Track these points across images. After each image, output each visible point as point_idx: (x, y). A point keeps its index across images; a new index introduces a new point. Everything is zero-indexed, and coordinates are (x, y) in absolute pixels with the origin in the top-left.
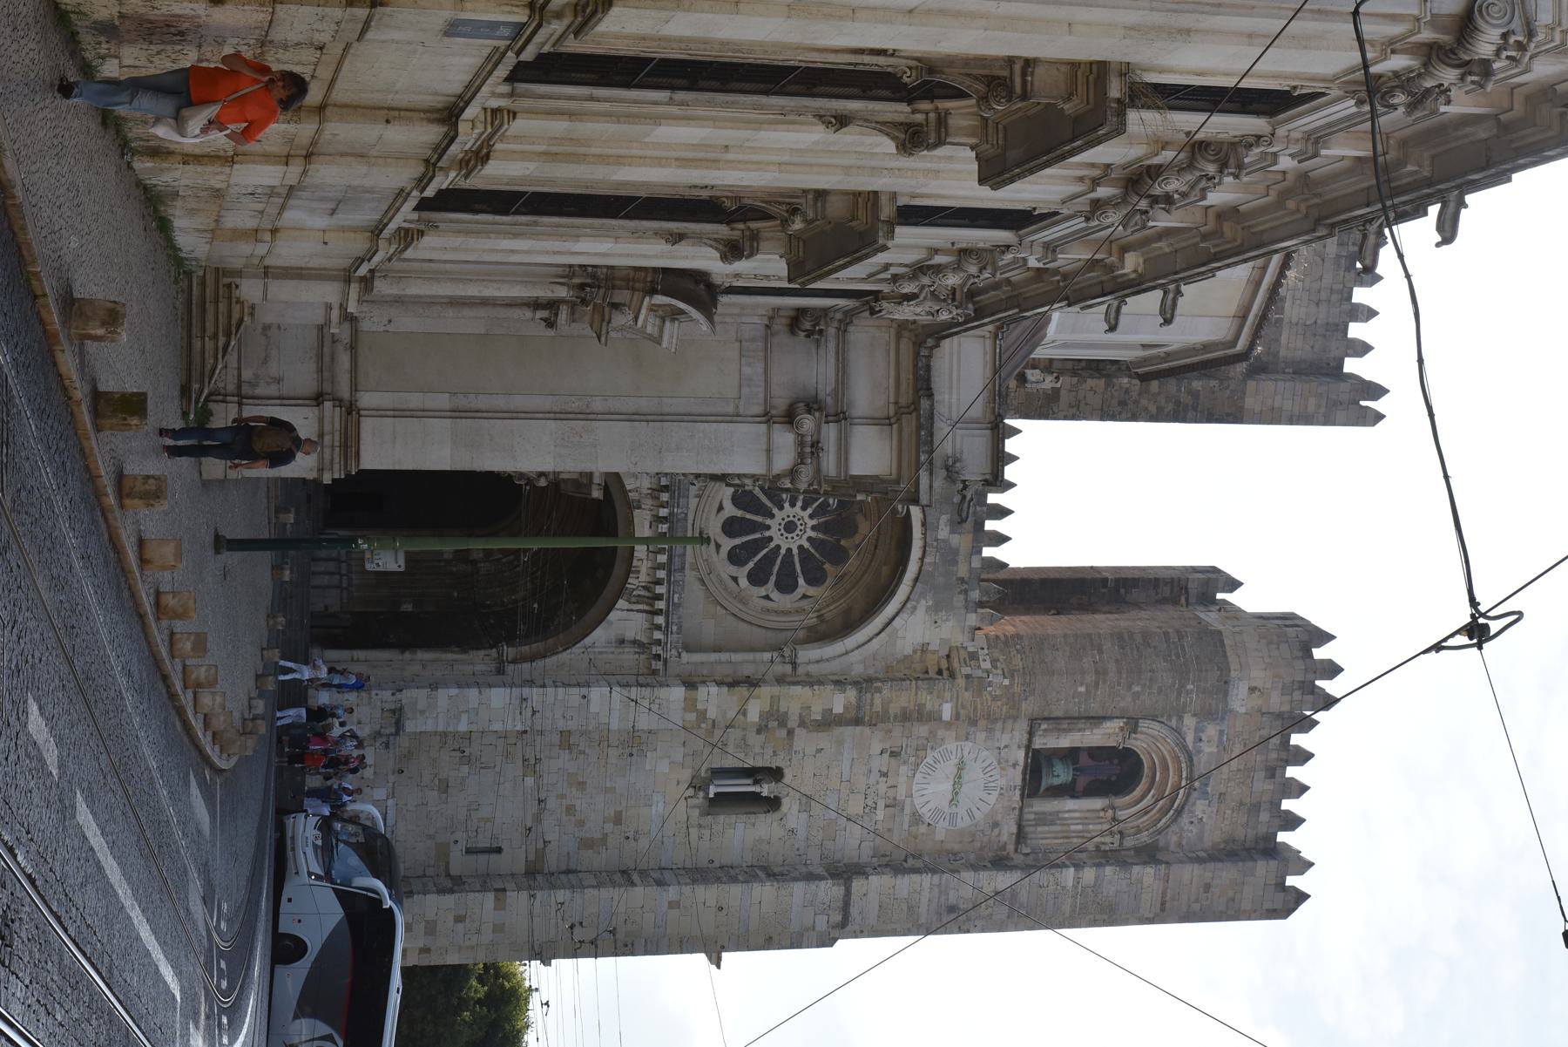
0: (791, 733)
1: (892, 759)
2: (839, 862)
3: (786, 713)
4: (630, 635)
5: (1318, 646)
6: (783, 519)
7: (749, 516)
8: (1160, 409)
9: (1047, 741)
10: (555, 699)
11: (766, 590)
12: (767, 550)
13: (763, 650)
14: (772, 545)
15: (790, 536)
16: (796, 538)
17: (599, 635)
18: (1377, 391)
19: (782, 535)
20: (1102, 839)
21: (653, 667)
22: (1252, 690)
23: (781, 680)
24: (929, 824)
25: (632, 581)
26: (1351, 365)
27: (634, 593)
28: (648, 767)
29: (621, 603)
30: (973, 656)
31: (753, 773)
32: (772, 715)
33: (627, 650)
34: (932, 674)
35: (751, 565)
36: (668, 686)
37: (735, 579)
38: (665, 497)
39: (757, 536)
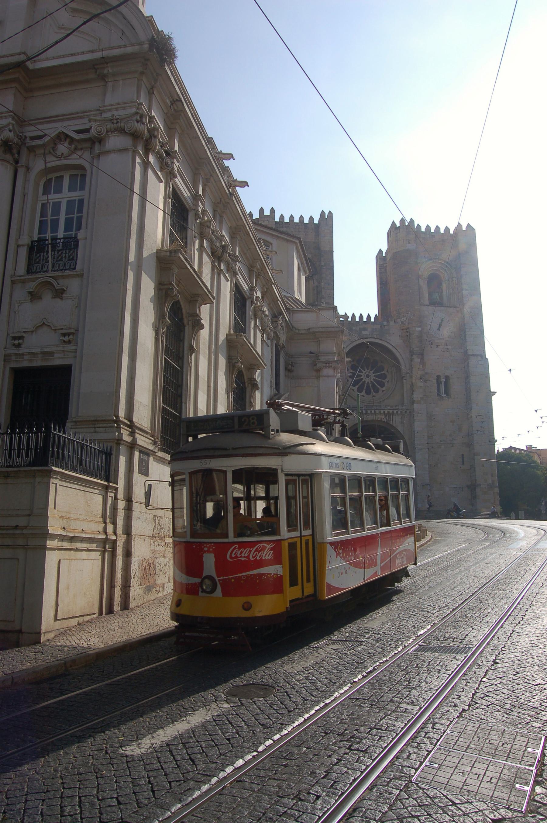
0: (426, 373)
5: (396, 225)
7: (365, 388)
9: (426, 301)
13: (403, 382)
17: (400, 429)
18: (323, 213)
22: (409, 243)
23: (411, 377)
25: (385, 420)
26: (316, 221)
30: (402, 322)
31: (439, 383)
34: (408, 334)
35: (379, 387)
37: (383, 391)
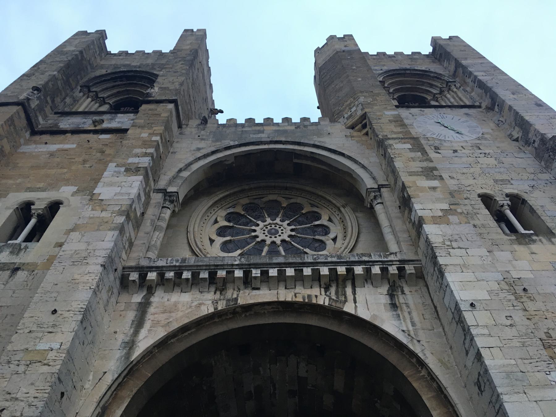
1: (442, 148)
2: (541, 166)
3: (422, 168)
4: (384, 299)
6: (266, 236)
8: (182, 64)
10: (490, 335)
11: (328, 240)
12: (292, 243)
14: (288, 239)
15: (280, 232)
16: (282, 228)
19: (280, 236)
20: (455, 90)
21: (413, 271)
24: (482, 134)
25: (323, 300)
27: (334, 297)
28: (532, 276)
29: (349, 308)
30: (351, 116)
32: (428, 174)
33: (402, 300)
36: (427, 238)
38: (222, 273)
39: (281, 249)
